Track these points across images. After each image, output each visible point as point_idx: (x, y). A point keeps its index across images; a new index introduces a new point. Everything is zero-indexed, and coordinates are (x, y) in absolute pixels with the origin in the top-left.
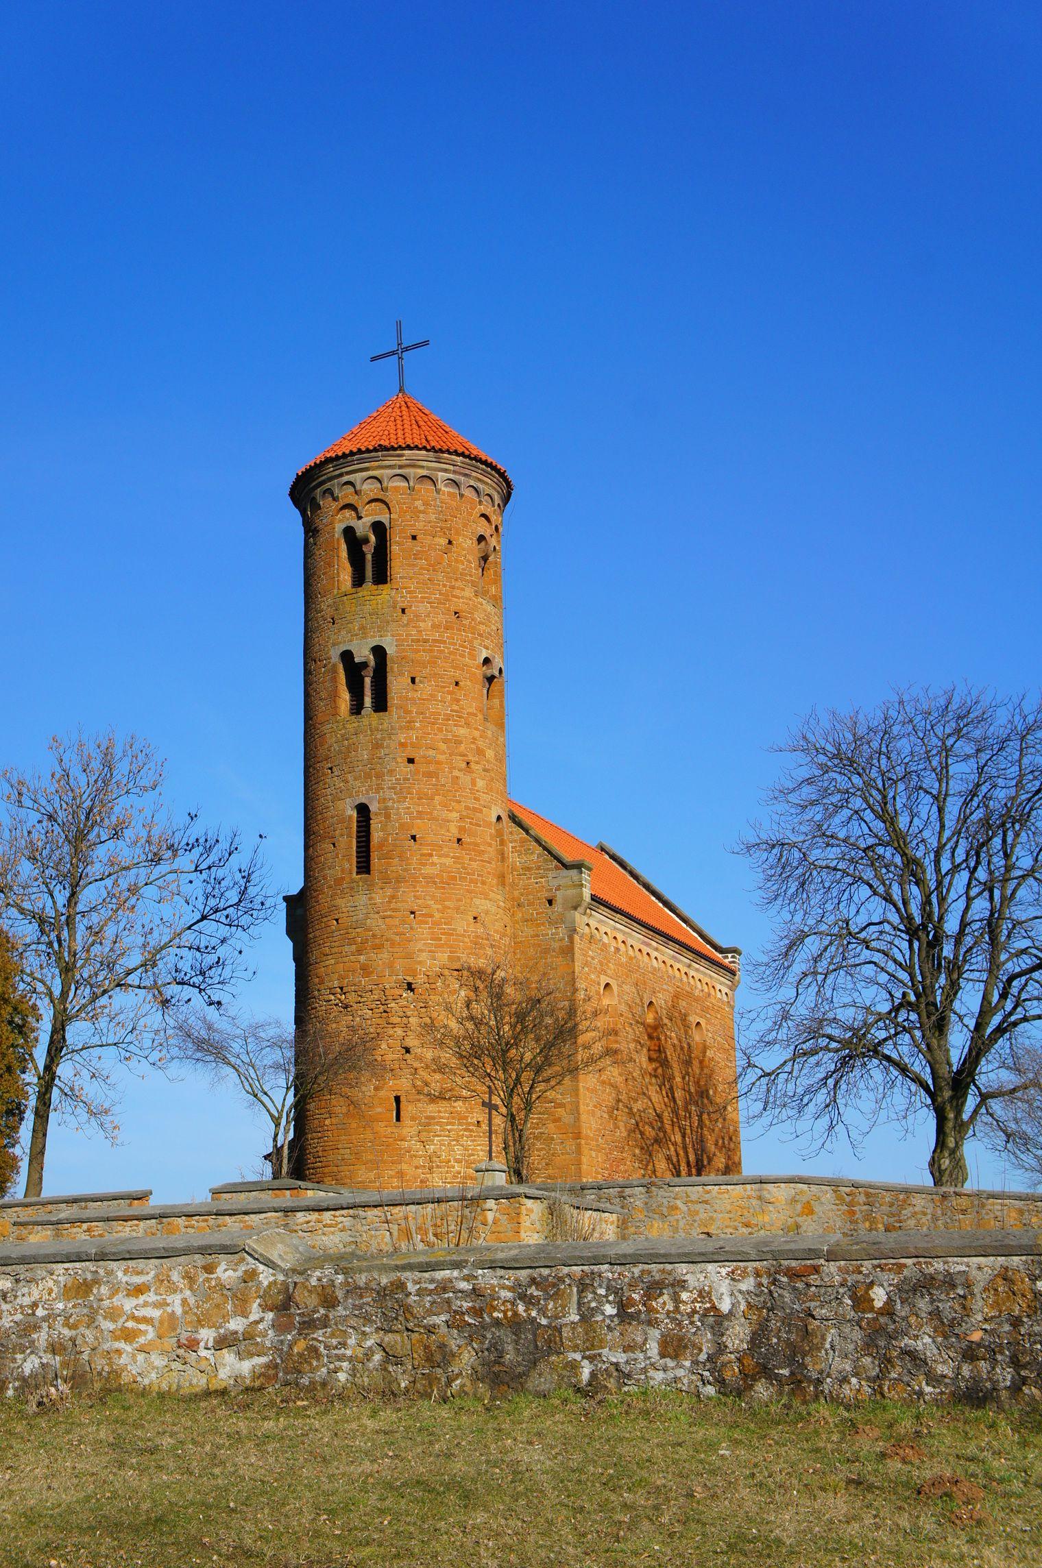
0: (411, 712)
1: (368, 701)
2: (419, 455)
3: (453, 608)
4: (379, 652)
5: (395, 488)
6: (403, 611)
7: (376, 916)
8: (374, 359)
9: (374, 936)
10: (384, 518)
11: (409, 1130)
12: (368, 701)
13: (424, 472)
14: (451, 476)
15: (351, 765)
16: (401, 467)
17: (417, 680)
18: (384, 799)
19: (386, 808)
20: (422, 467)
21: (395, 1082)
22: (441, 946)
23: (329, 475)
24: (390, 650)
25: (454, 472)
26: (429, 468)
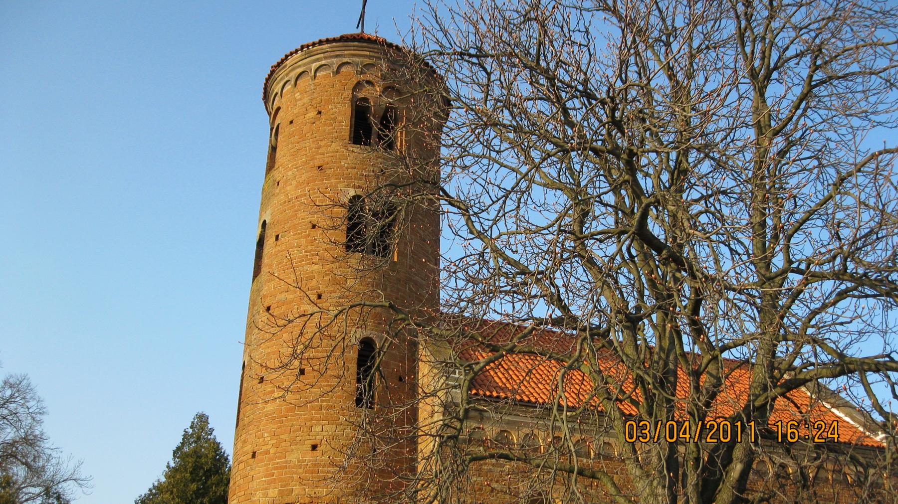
3: (317, 163)
14: (324, 62)
22: (273, 481)
25: (326, 58)
26: (304, 65)
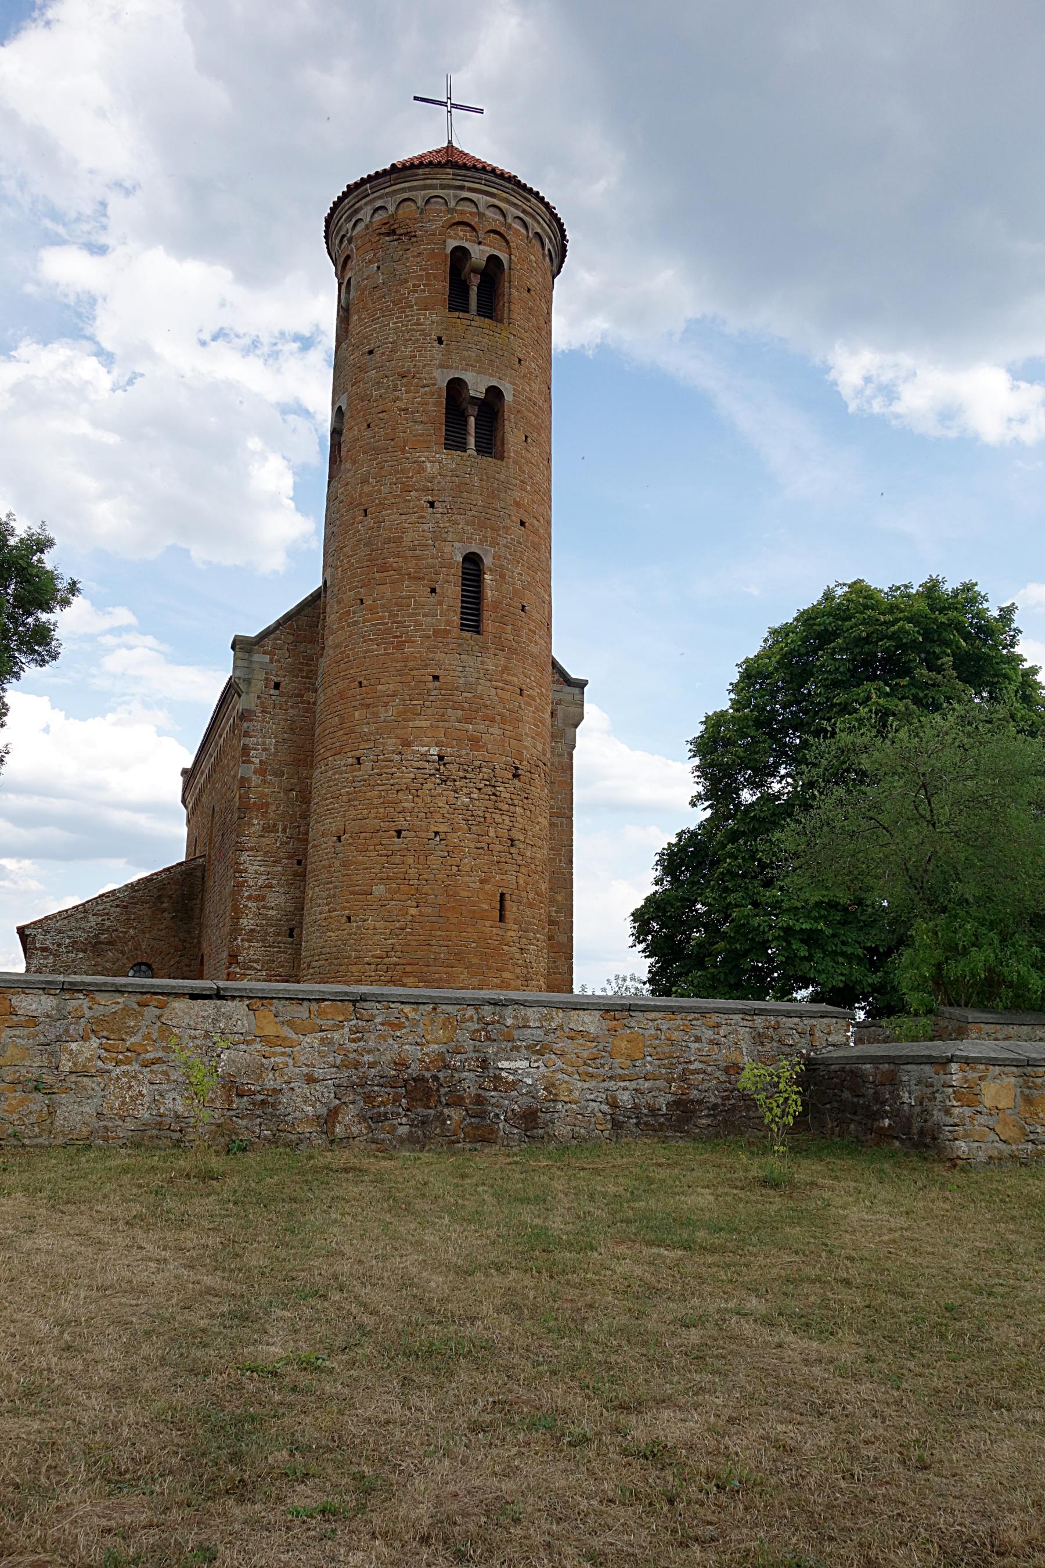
0: (523, 472)
1: (472, 441)
2: (540, 209)
4: (494, 393)
5: (516, 229)
6: (520, 360)
7: (489, 684)
8: (416, 98)
9: (485, 706)
10: (504, 257)
11: (513, 934)
12: (472, 441)
13: (539, 231)
15: (462, 506)
16: (524, 211)
17: (529, 440)
18: (500, 556)
19: (501, 567)
20: (539, 223)
21: (502, 877)
23: (445, 182)
24: (508, 397)
26: (542, 228)
